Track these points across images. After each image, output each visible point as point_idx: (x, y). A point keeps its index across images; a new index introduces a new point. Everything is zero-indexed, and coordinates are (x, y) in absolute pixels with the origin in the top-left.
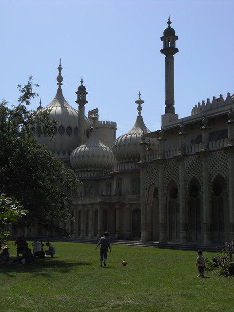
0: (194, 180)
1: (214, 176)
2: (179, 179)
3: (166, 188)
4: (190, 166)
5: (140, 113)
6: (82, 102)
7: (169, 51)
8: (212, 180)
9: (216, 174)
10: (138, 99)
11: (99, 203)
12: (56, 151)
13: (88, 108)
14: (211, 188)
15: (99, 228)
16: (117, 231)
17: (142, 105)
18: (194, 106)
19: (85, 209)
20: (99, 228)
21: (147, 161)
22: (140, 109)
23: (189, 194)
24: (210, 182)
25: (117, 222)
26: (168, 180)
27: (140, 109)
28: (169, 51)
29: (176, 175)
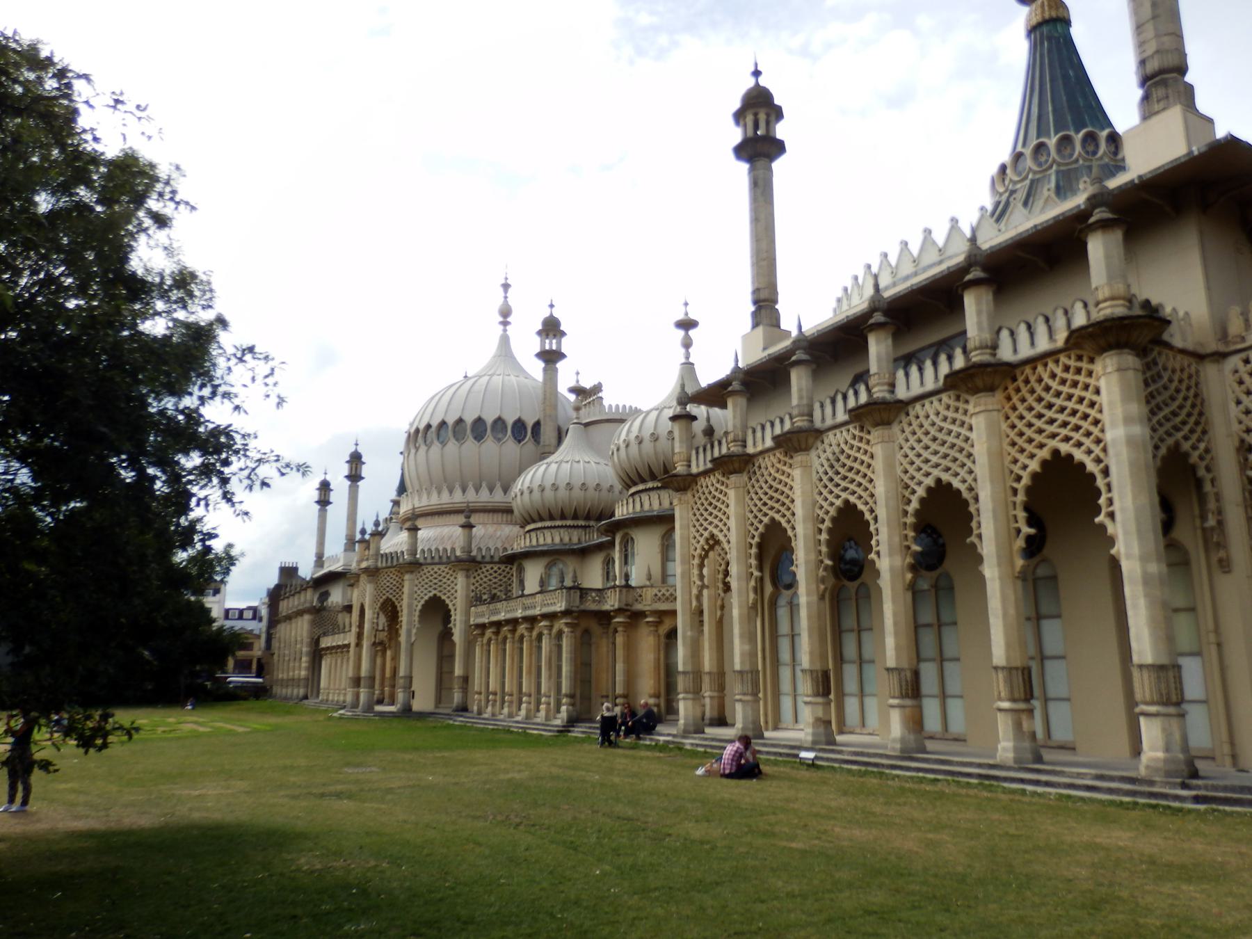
0: (849, 508)
1: (921, 492)
2: (793, 514)
3: (754, 551)
4: (832, 466)
5: (688, 356)
6: (551, 358)
7: (760, 149)
8: (915, 505)
9: (930, 481)
10: (681, 316)
11: (566, 613)
12: (484, 485)
13: (566, 377)
14: (911, 534)
15: (565, 689)
16: (620, 696)
17: (692, 333)
18: (840, 294)
19: (535, 633)
20: (565, 689)
21: (694, 470)
22: (687, 344)
23: (829, 562)
24: (906, 513)
25: (620, 667)
26: (761, 522)
27: (687, 344)
28: (760, 149)
29: (784, 504)
